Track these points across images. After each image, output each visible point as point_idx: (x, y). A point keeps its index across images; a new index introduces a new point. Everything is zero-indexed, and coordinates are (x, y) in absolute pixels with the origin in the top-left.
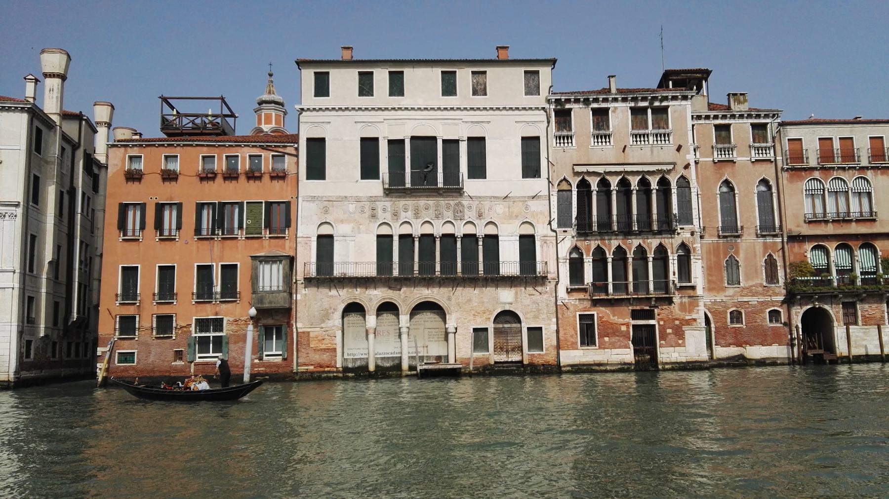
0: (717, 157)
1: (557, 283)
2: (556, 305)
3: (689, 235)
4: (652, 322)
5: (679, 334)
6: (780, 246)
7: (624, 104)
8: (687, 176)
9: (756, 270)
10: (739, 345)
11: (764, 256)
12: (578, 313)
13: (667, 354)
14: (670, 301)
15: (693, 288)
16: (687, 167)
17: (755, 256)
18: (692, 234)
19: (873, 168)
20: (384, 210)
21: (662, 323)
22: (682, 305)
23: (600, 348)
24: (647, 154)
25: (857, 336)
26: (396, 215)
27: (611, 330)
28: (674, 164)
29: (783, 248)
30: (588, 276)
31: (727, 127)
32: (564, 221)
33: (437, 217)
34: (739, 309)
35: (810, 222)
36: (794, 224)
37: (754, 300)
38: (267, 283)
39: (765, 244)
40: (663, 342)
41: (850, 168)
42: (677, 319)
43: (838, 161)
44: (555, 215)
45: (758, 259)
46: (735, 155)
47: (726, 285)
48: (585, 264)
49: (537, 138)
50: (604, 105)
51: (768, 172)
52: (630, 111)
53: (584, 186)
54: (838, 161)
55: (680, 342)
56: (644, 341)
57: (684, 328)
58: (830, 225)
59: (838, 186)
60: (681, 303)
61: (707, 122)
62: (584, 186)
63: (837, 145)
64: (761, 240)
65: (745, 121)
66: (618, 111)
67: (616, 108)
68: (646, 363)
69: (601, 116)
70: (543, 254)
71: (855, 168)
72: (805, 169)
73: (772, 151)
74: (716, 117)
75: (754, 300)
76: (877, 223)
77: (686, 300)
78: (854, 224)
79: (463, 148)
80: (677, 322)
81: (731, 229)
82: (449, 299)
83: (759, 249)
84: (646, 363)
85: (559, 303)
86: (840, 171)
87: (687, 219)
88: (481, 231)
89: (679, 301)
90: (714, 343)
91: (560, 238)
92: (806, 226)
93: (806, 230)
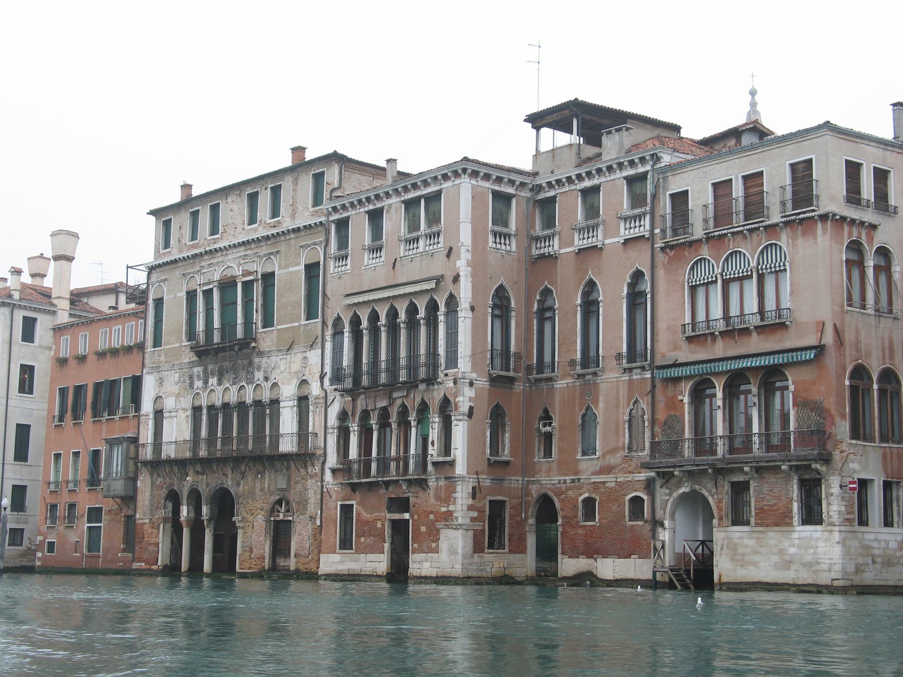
0: (579, 242)
1: (324, 462)
2: (322, 492)
3: (451, 384)
4: (407, 516)
5: (434, 535)
6: (649, 388)
7: (398, 199)
8: (456, 294)
9: (617, 428)
10: (589, 555)
11: (628, 405)
12: (339, 503)
13: (420, 564)
14: (422, 484)
15: (452, 464)
16: (456, 279)
17: (617, 406)
18: (455, 383)
19: (786, 224)
20: (198, 376)
21: (416, 517)
22: (437, 489)
23: (356, 552)
24: (417, 265)
25: (746, 546)
26: (206, 382)
27: (368, 529)
28: (439, 280)
29: (654, 386)
30: (353, 453)
31: (596, 189)
32: (337, 377)
33: (234, 383)
34: (593, 496)
35: (690, 339)
36: (669, 345)
37: (610, 480)
38: (114, 470)
39: (631, 381)
40: (416, 545)
41: (751, 231)
42: (432, 513)
43: (739, 219)
44: (328, 369)
45: (621, 411)
46: (600, 238)
47: (579, 457)
48: (352, 434)
49: (318, 263)
50: (379, 205)
51: (640, 260)
52: (403, 206)
53: (356, 322)
54: (739, 219)
55: (434, 545)
56: (401, 543)
57: (439, 525)
58: (720, 342)
59: (736, 269)
60: (437, 487)
61: (573, 187)
62: (356, 322)
63: (738, 190)
64: (626, 378)
65: (618, 175)
66: (393, 210)
67: (390, 206)
68: (398, 574)
69: (376, 217)
70: (315, 423)
71: (758, 228)
72: (691, 243)
73: (648, 218)
74: (579, 177)
75: (610, 480)
76: (792, 330)
77: (442, 483)
78: (720, 342)
79: (258, 289)
80: (432, 517)
81: (589, 359)
82: (238, 485)
83: (623, 392)
84: (398, 574)
85: (325, 490)
86: (739, 238)
87: (452, 361)
88: (266, 396)
89: (435, 484)
90: (560, 551)
91: (330, 399)
92: (685, 346)
93: (685, 354)
